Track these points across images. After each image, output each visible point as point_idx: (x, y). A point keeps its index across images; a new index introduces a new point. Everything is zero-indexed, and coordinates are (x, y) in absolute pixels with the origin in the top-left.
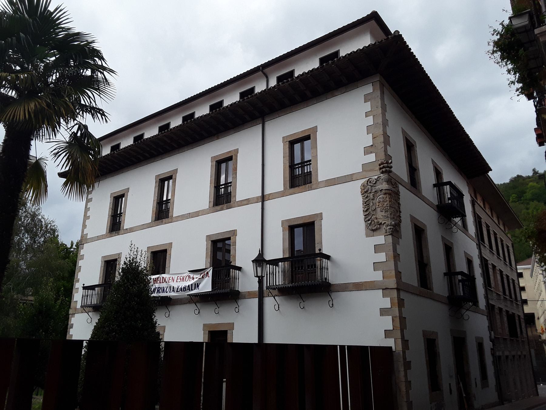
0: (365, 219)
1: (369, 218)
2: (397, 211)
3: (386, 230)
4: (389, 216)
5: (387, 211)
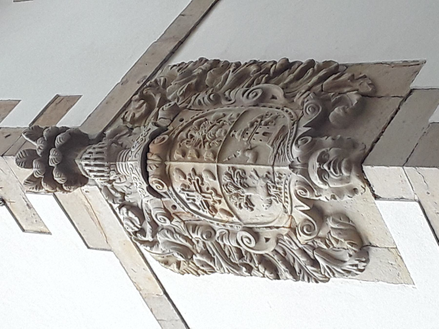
0: (310, 277)
1: (303, 260)
2: (264, 98)
3: (337, 194)
4: (263, 169)
5: (243, 175)
